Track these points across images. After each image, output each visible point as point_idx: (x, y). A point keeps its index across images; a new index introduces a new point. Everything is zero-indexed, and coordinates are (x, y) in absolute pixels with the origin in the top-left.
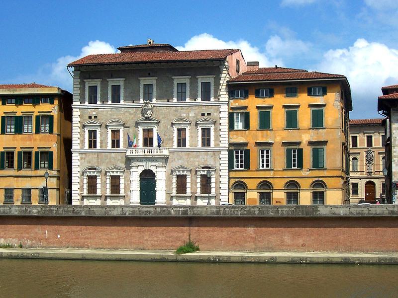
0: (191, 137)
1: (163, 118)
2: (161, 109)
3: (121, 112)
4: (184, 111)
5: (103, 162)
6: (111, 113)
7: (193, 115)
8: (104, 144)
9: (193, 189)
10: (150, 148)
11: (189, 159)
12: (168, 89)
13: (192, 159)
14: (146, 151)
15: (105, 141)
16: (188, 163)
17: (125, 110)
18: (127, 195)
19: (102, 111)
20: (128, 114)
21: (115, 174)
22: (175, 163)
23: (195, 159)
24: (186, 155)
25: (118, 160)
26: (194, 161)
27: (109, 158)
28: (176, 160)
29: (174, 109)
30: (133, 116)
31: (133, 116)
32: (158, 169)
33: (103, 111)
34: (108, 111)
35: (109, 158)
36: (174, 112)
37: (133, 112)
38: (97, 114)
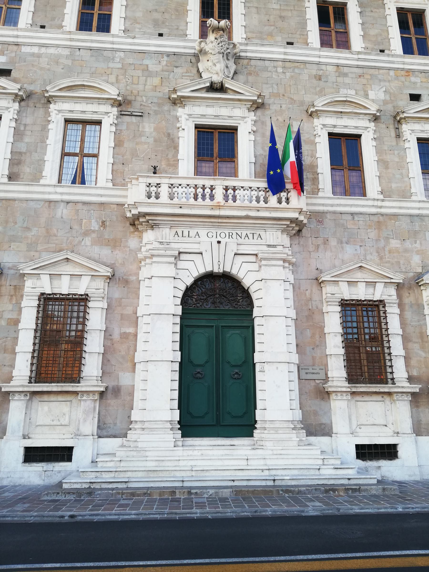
0: (382, 163)
1: (276, 95)
2: (266, 69)
3: (111, 65)
4: (347, 80)
5: (13, 239)
6: (69, 62)
7: (382, 96)
8: (26, 170)
9: (413, 362)
10: (231, 182)
11: (382, 243)
12: (289, 14)
13: (395, 243)
14: (219, 193)
15: (36, 156)
16: (381, 258)
17: (131, 61)
18: (116, 391)
19: (33, 55)
20: (139, 73)
21: (64, 287)
22: (328, 254)
23: (408, 244)
24: (370, 226)
25: (86, 233)
26: (406, 251)
27: (43, 220)
28: (333, 242)
29: (314, 72)
30: (156, 81)
31: (156, 81)
32: (266, 273)
33: (39, 56)
34: (60, 56)
35: (43, 220)
36: (315, 81)
37: (158, 68)
38: (12, 61)
